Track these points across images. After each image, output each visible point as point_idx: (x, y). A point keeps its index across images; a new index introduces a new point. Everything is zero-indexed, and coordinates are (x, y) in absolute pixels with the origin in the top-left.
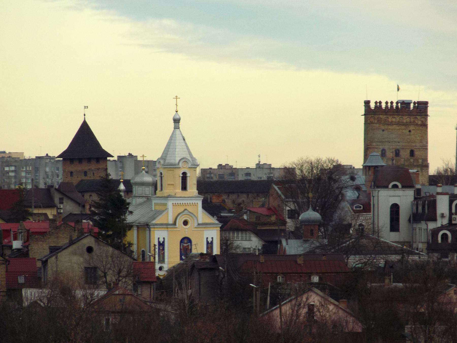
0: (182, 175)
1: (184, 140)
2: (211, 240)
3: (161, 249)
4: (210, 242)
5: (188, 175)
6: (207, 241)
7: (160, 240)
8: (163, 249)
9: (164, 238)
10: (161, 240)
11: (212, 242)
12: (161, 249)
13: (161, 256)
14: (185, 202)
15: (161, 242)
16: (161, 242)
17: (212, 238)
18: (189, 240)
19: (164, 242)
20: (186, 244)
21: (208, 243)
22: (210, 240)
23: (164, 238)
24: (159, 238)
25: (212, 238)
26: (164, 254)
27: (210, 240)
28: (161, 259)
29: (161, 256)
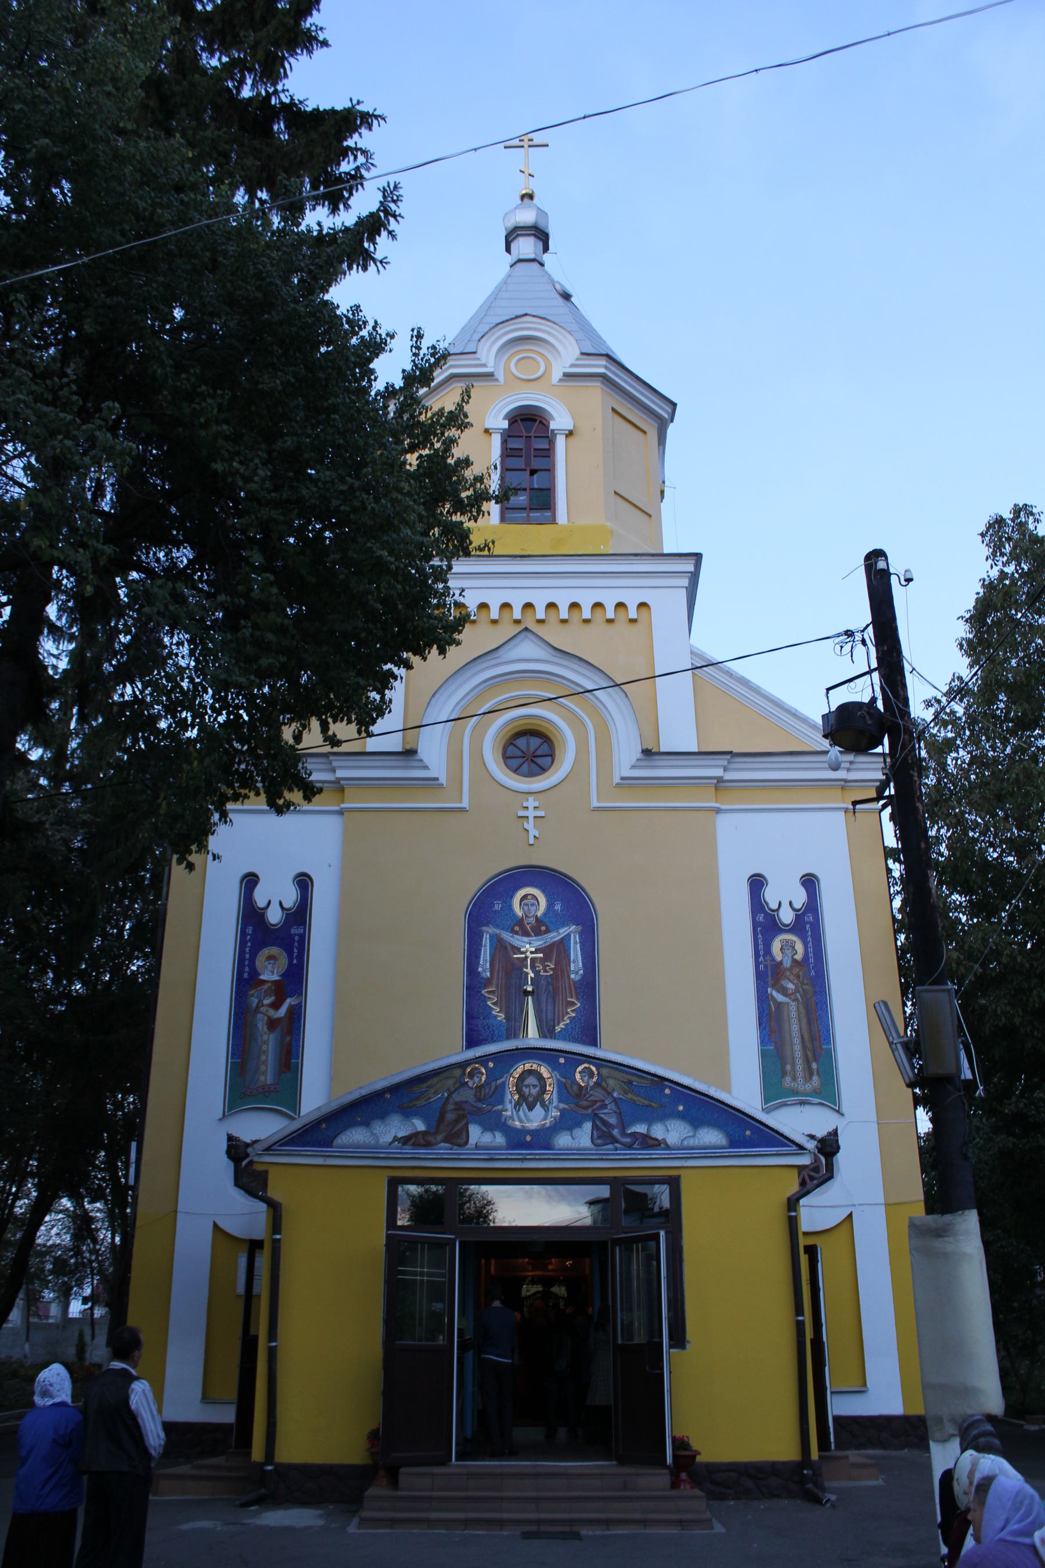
0: (505, 425)
1: (566, 296)
2: (800, 898)
3: (270, 974)
4: (787, 916)
5: (560, 420)
6: (757, 903)
7: (260, 897)
8: (294, 979)
9: (304, 882)
10: (276, 896)
11: (809, 922)
12: (270, 974)
13: (269, 1044)
14: (528, 597)
15: (274, 916)
16: (274, 916)
17: (809, 882)
18: (571, 899)
19: (299, 915)
20: (539, 927)
21: (765, 924)
22: (785, 896)
23: (304, 882)
24: (250, 881)
25: (809, 882)
26: (292, 1026)
27: (785, 896)
28: (267, 1075)
29: (269, 1044)
